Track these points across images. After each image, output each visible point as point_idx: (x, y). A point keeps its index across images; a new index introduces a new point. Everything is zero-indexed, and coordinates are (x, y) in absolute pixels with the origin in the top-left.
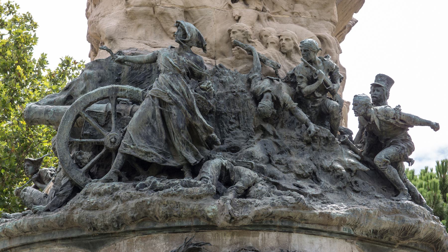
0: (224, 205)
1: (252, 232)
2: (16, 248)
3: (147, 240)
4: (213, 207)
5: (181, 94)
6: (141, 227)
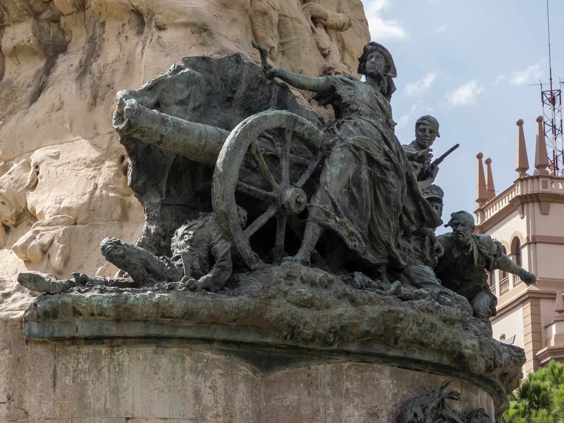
2: (129, 340)
3: (366, 371)
6: (367, 350)
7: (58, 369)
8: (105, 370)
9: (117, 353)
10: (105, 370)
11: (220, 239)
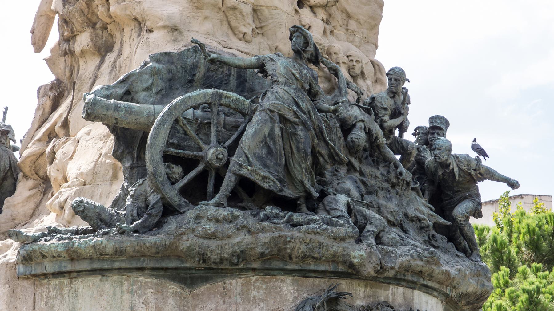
0: (370, 252)
1: (383, 285)
3: (270, 281)
4: (361, 253)
6: (267, 266)
7: (37, 298)
8: (66, 296)
9: (74, 283)
10: (66, 296)
11: (153, 192)
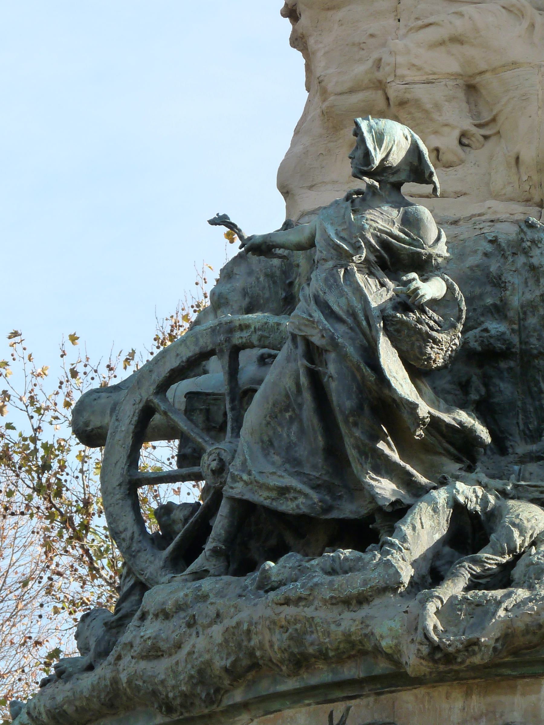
4: (392, 624)
5: (350, 321)
